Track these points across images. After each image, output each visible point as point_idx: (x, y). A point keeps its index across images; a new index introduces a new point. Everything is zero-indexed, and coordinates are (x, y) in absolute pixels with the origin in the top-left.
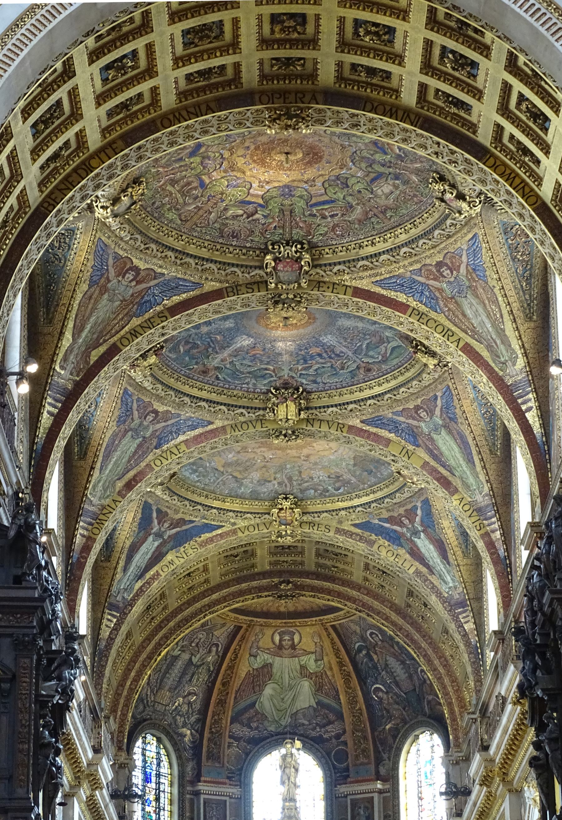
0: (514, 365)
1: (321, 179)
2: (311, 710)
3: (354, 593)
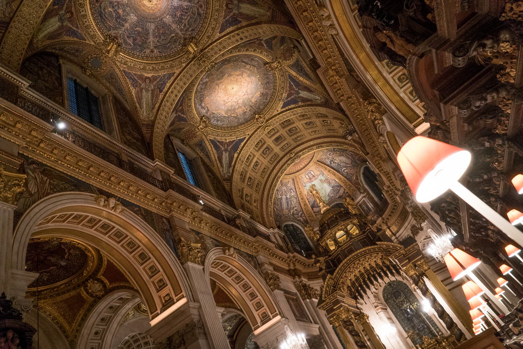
2: (332, 191)
3: (312, 143)
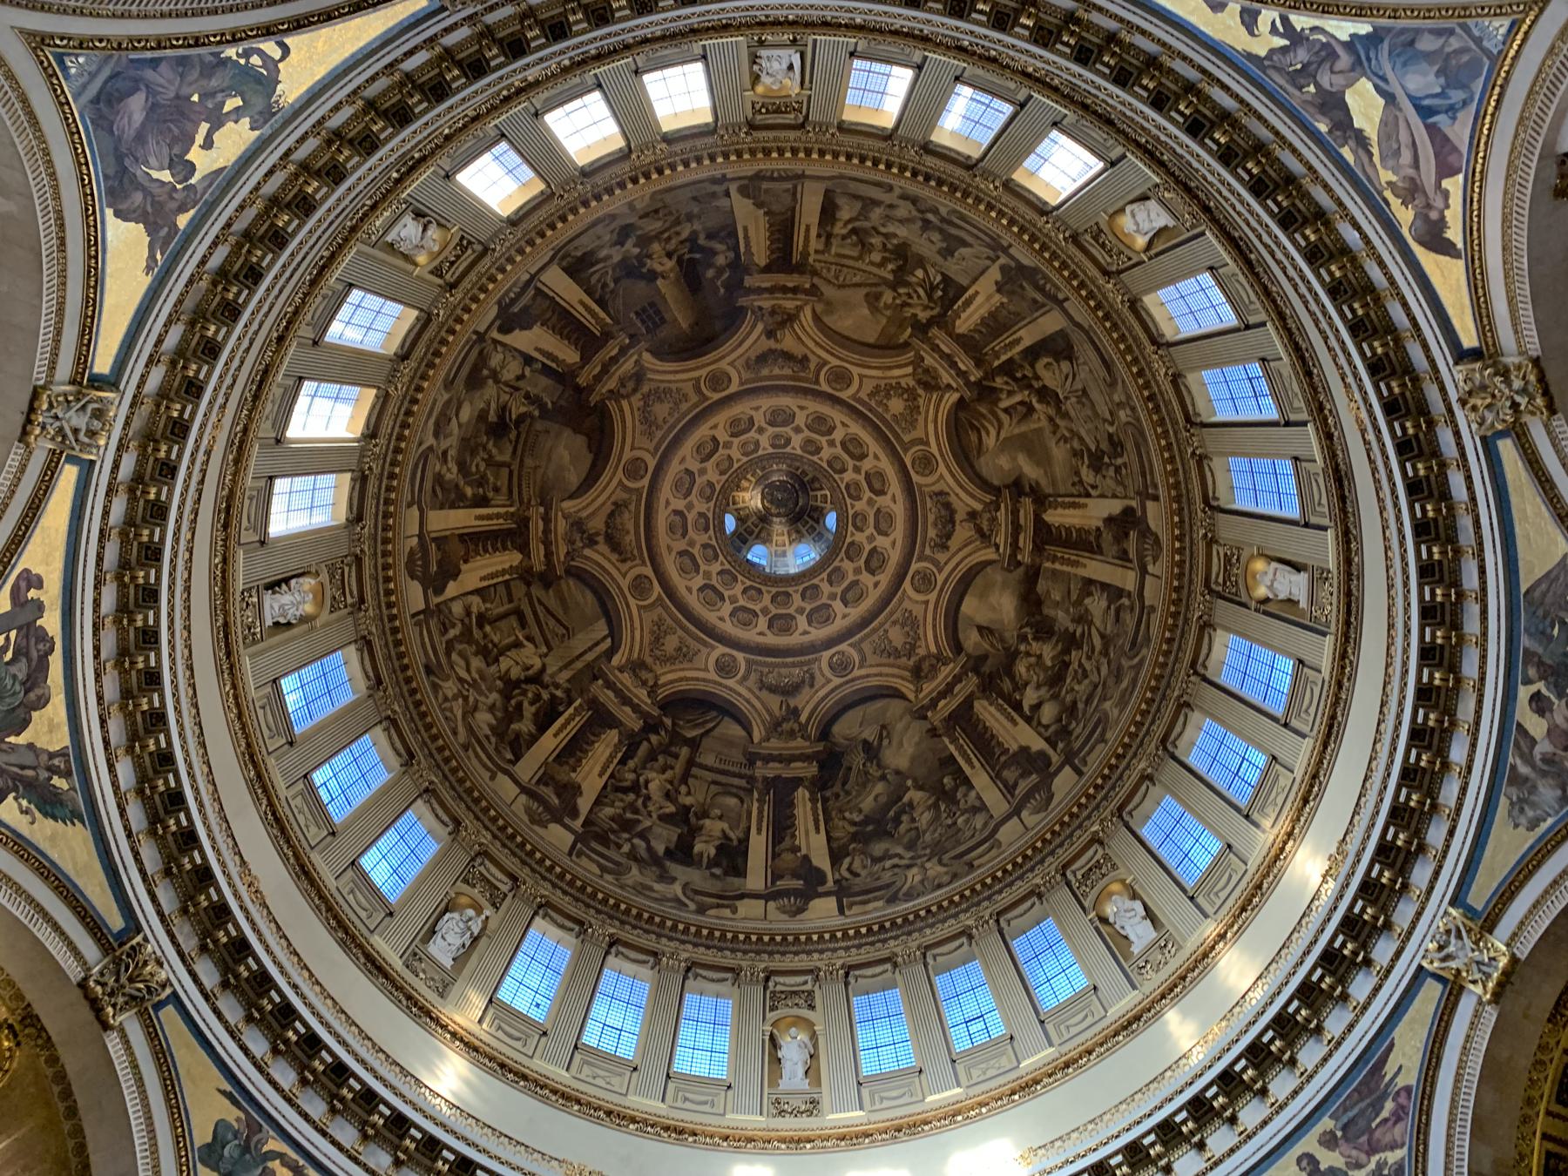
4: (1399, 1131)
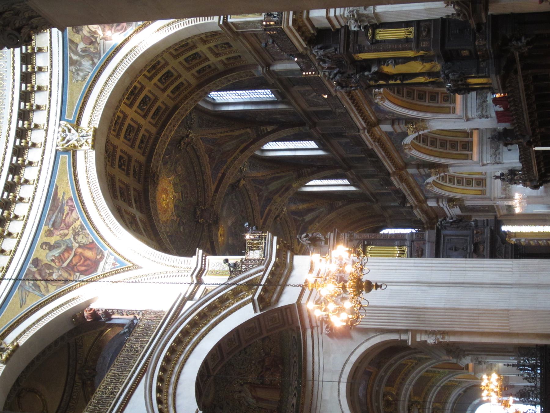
0: (249, 133)
1: (173, 192)
4: (74, 215)
